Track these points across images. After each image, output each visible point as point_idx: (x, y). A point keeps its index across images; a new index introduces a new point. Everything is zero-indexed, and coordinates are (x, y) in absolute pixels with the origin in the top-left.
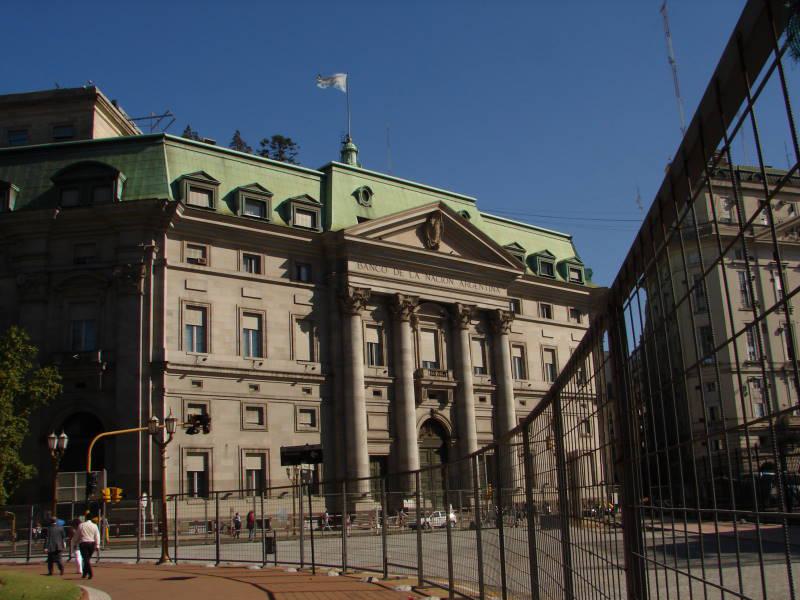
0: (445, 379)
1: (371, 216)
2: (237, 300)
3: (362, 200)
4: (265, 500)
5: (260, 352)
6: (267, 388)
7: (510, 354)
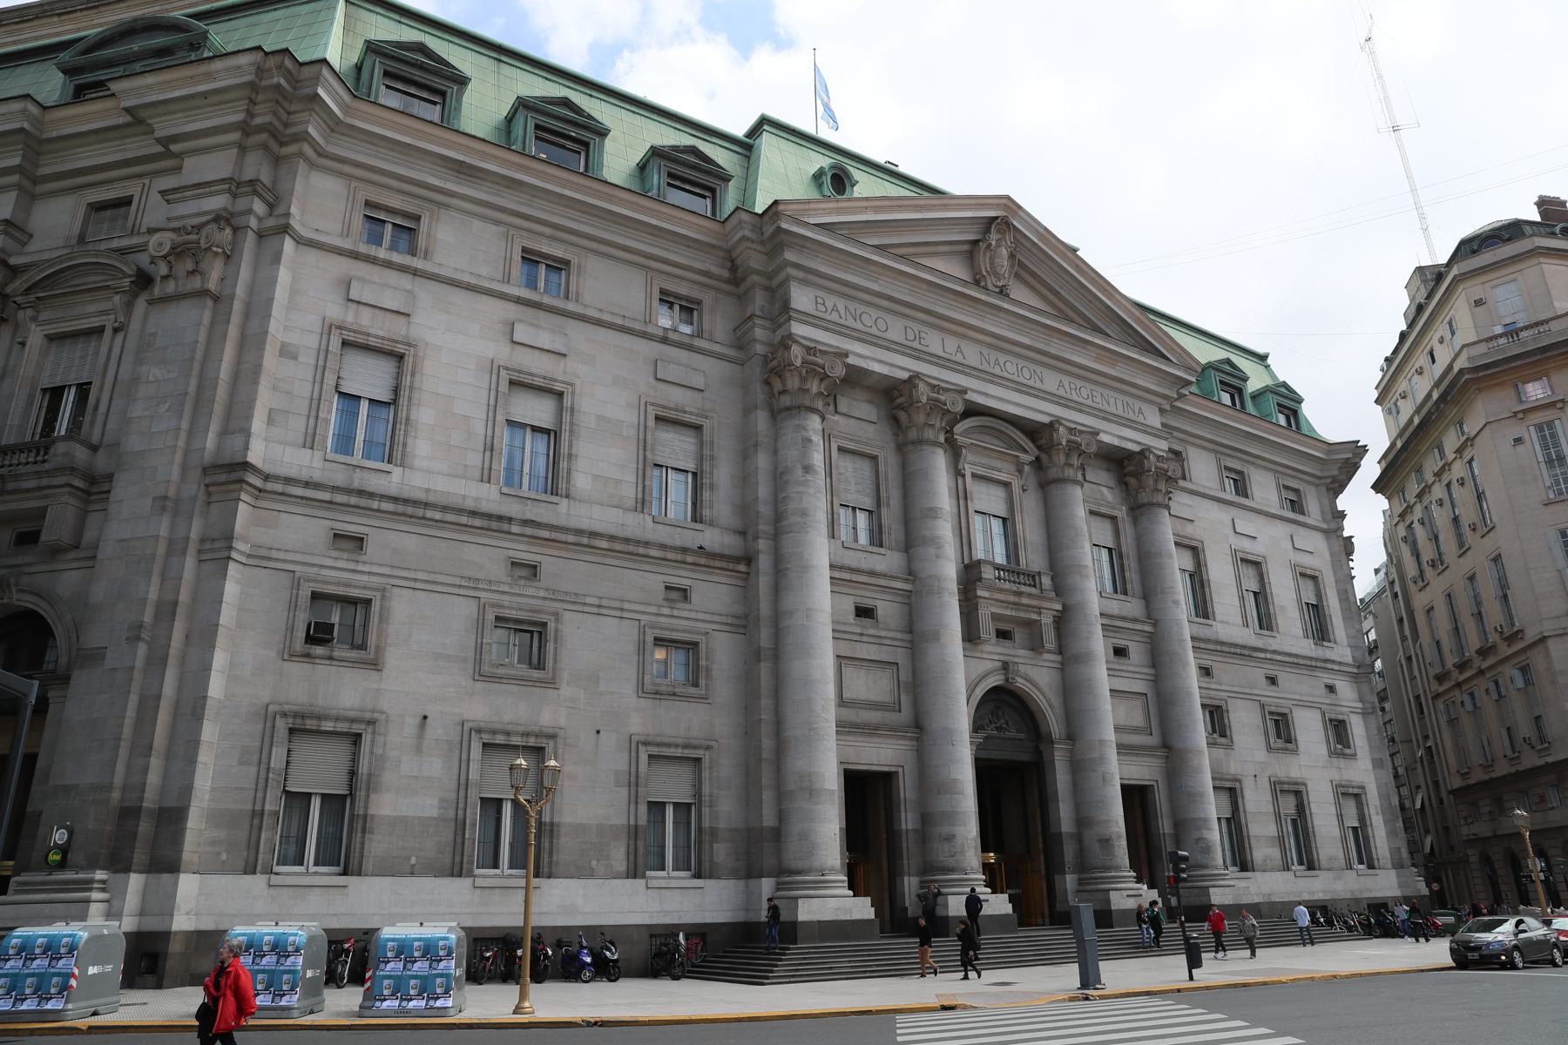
0: (1033, 590)
2: (501, 352)
4: (535, 882)
5: (555, 483)
7: (1176, 565)
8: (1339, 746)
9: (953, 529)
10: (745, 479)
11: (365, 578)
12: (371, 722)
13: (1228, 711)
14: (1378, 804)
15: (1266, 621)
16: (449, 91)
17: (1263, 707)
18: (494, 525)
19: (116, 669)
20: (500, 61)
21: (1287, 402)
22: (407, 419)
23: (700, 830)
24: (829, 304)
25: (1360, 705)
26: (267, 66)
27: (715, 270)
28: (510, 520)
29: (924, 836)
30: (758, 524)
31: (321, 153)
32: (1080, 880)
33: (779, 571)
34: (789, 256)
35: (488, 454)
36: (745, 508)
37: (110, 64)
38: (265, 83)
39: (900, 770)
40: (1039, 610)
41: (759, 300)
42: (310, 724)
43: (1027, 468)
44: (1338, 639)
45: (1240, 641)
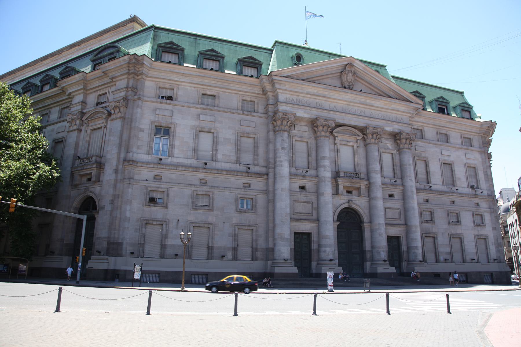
10: (267, 152)
12: (165, 221)
13: (433, 213)
14: (493, 242)
16: (179, 53)
17: (448, 211)
19: (107, 211)
20: (196, 39)
25: (489, 209)
26: (131, 58)
29: (319, 251)
32: (372, 263)
33: (275, 177)
35: (194, 151)
36: (267, 160)
37: (101, 58)
38: (131, 62)
39: (312, 232)
42: (151, 222)
43: (359, 141)
44: (482, 188)
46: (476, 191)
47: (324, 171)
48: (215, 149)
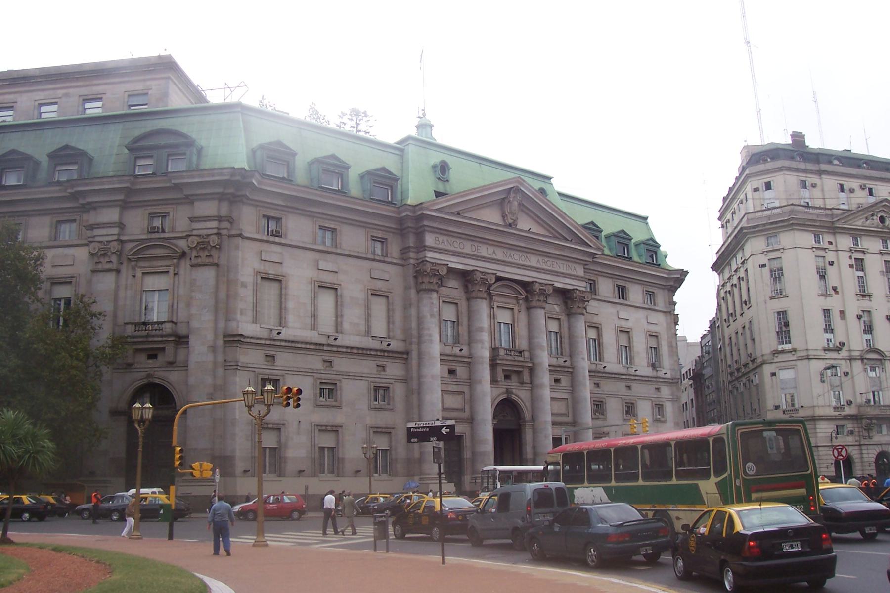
0: (521, 359)
1: (449, 190)
3: (439, 175)
6: (342, 364)
8: (659, 417)
9: (488, 335)
10: (406, 318)
11: (276, 371)
12: (284, 424)
15: (630, 360)
17: (623, 400)
18: (318, 347)
21: (652, 248)
22: (285, 307)
23: (391, 459)
24: (441, 239)
25: (671, 397)
27: (393, 226)
28: (323, 345)
29: (473, 460)
30: (412, 339)
31: (248, 198)
34: (426, 223)
36: (406, 330)
40: (523, 367)
41: (411, 241)
45: (615, 371)
46: (657, 371)
47: (482, 348)
48: (339, 313)
